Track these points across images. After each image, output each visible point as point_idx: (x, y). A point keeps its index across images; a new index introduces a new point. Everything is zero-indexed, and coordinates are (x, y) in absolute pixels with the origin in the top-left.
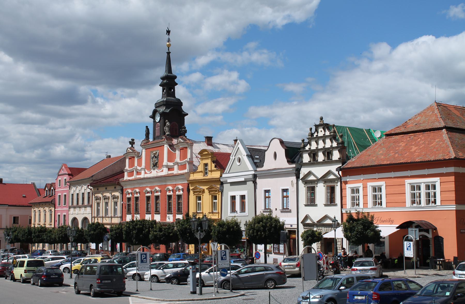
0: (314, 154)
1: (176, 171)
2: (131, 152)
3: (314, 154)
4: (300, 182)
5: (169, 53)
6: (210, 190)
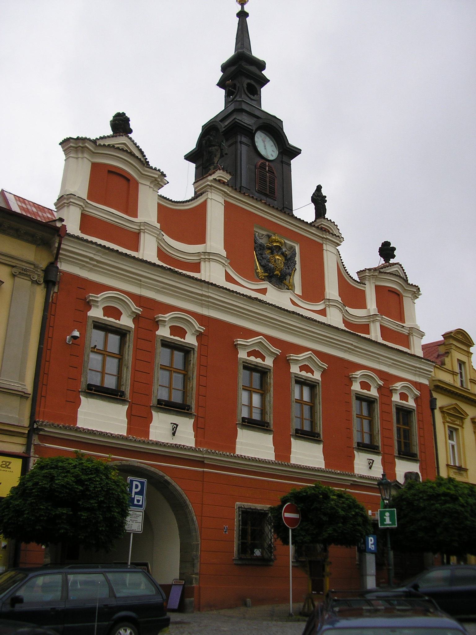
5: (243, 15)
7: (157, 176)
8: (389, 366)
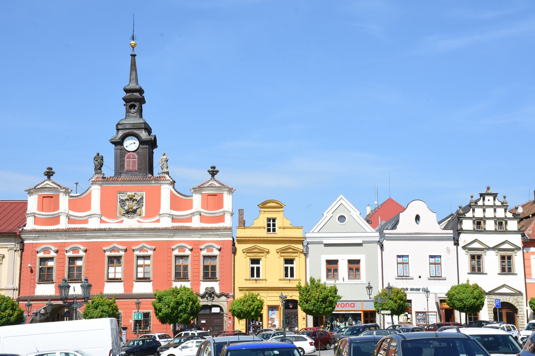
0: (479, 223)
1: (196, 223)
2: (55, 188)
3: (479, 223)
4: (460, 248)
6: (281, 251)
7: (64, 191)
8: (200, 237)
